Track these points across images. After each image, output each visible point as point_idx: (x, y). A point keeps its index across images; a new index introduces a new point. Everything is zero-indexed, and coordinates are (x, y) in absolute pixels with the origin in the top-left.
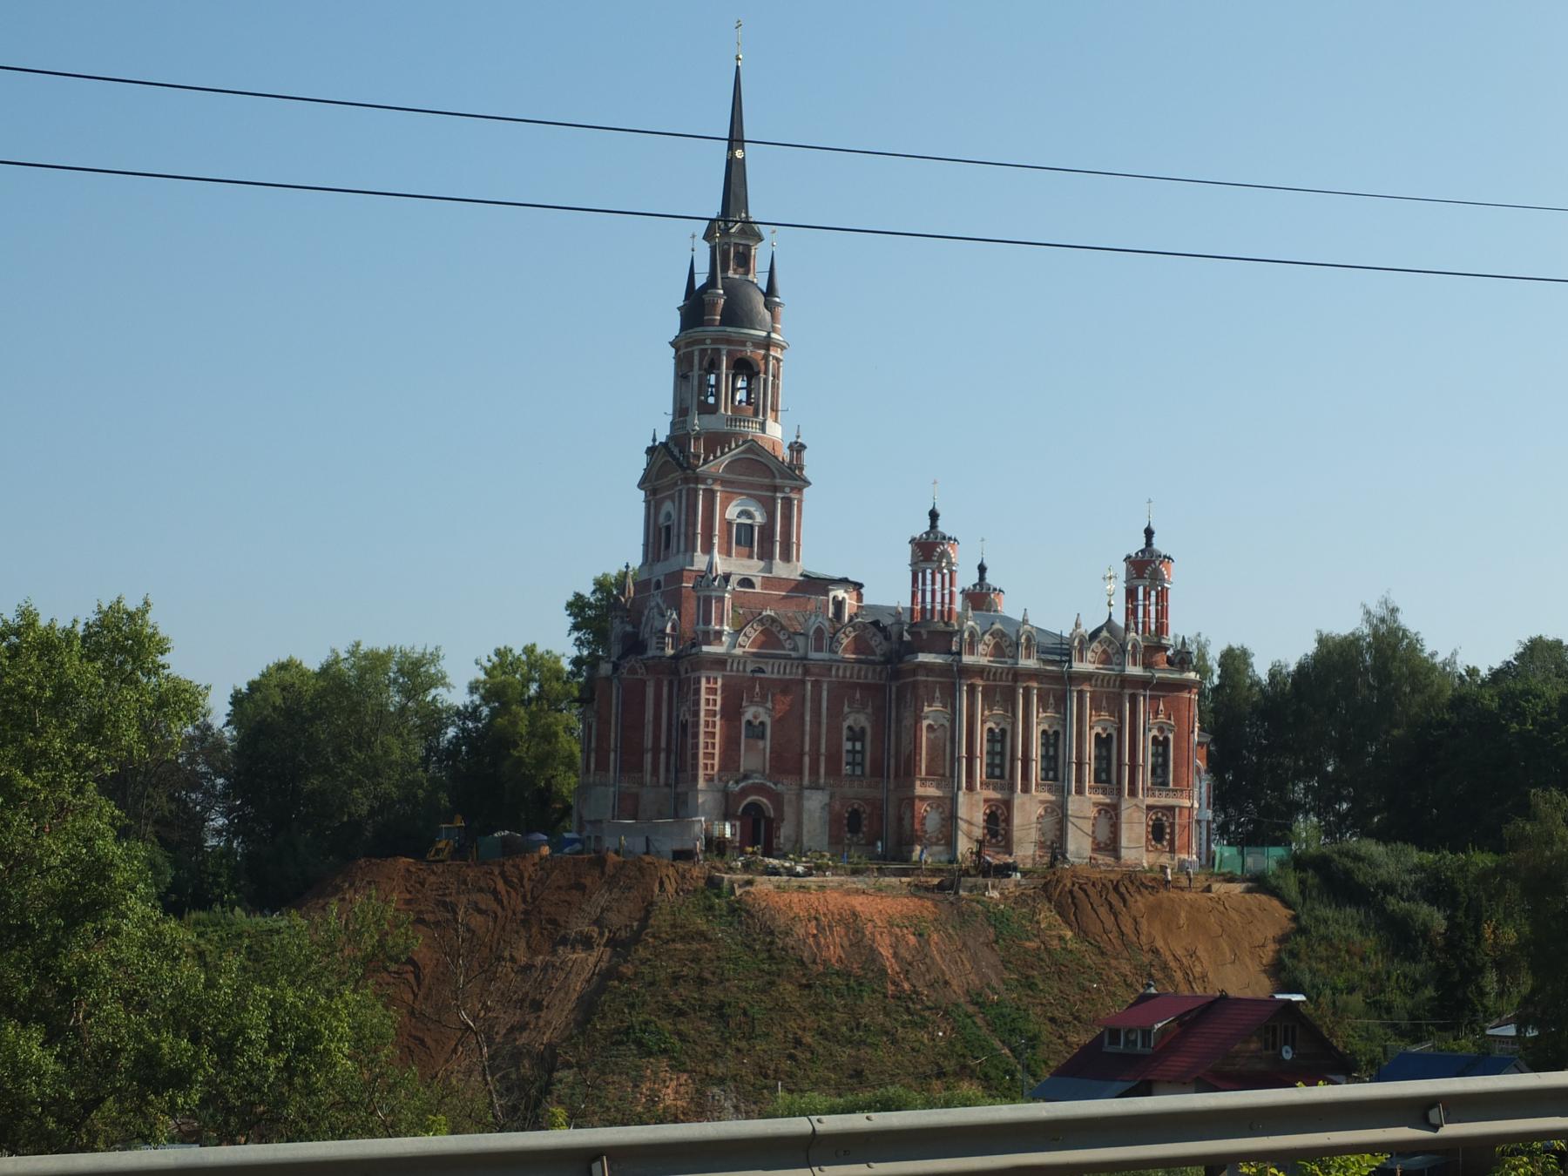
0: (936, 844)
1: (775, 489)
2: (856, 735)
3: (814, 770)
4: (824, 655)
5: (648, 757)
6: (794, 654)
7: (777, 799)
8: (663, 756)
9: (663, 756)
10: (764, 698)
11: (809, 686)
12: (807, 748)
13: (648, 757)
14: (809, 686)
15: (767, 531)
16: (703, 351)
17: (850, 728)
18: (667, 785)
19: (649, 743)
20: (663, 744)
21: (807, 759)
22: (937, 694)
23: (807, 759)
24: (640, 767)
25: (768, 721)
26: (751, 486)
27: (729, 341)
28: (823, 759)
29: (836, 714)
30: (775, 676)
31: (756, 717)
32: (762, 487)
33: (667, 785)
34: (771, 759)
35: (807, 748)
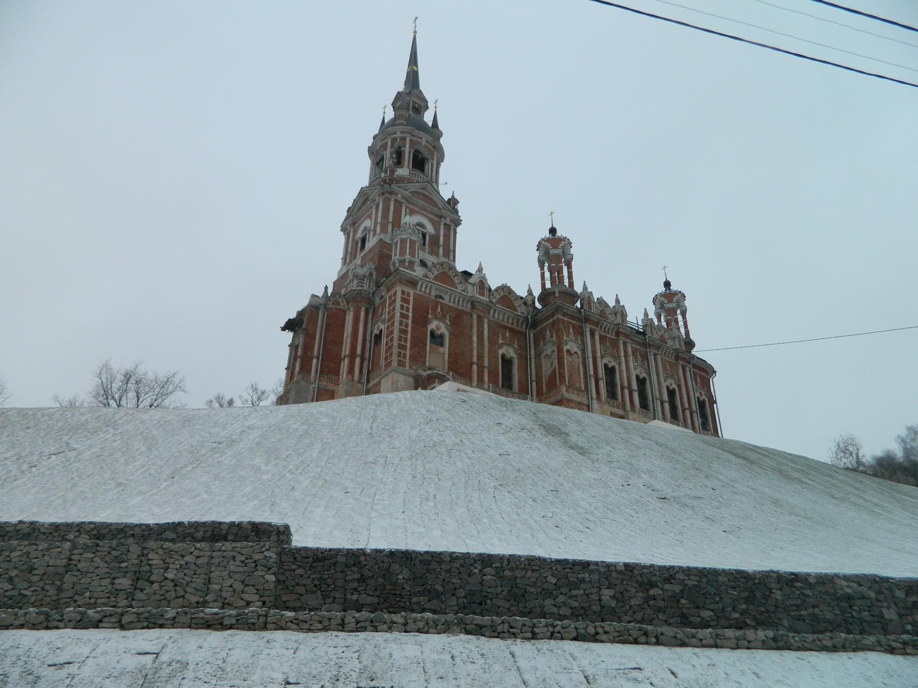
1: (441, 217)
5: (345, 364)
8: (358, 361)
9: (358, 361)
10: (444, 316)
12: (475, 360)
13: (345, 364)
16: (394, 140)
18: (359, 382)
19: (346, 350)
20: (359, 351)
21: (475, 367)
23: (475, 367)
24: (337, 372)
28: (486, 370)
30: (452, 304)
31: (438, 328)
33: (359, 382)
34: (449, 362)
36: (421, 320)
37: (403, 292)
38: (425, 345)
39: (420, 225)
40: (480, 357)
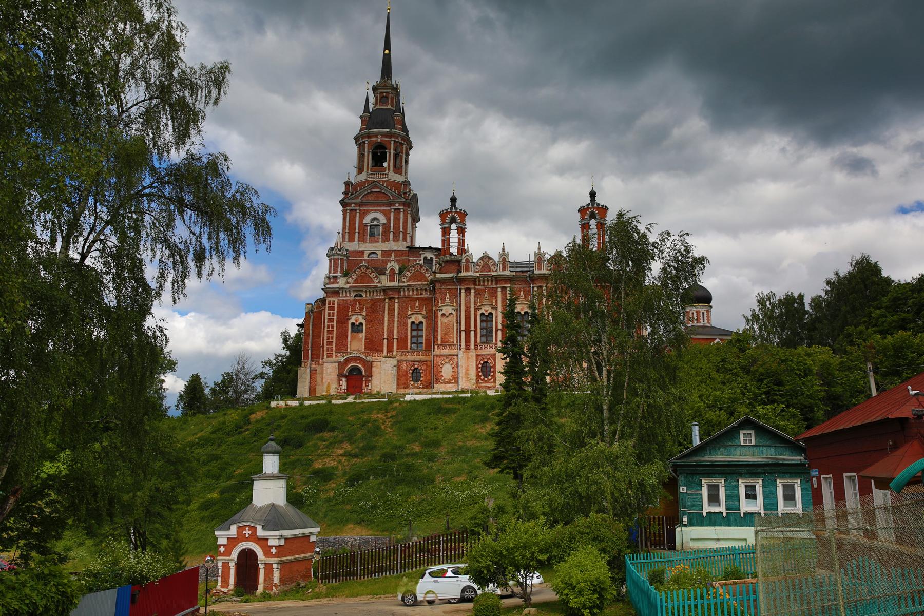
0: (448, 383)
1: (391, 204)
2: (417, 327)
3: (390, 347)
4: (396, 284)
6: (379, 285)
7: (369, 366)
10: (361, 309)
11: (387, 301)
12: (385, 336)
14: (387, 301)
15: (386, 227)
17: (413, 323)
21: (385, 341)
22: (448, 296)
23: (385, 341)
25: (364, 322)
26: (378, 204)
27: (369, 136)
29: (403, 316)
32: (384, 205)
35: (385, 336)
36: (343, 319)
37: (330, 303)
38: (347, 336)
39: (375, 219)
40: (391, 331)
